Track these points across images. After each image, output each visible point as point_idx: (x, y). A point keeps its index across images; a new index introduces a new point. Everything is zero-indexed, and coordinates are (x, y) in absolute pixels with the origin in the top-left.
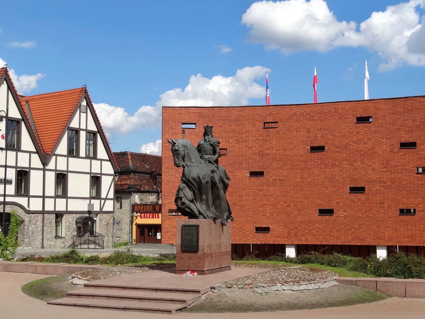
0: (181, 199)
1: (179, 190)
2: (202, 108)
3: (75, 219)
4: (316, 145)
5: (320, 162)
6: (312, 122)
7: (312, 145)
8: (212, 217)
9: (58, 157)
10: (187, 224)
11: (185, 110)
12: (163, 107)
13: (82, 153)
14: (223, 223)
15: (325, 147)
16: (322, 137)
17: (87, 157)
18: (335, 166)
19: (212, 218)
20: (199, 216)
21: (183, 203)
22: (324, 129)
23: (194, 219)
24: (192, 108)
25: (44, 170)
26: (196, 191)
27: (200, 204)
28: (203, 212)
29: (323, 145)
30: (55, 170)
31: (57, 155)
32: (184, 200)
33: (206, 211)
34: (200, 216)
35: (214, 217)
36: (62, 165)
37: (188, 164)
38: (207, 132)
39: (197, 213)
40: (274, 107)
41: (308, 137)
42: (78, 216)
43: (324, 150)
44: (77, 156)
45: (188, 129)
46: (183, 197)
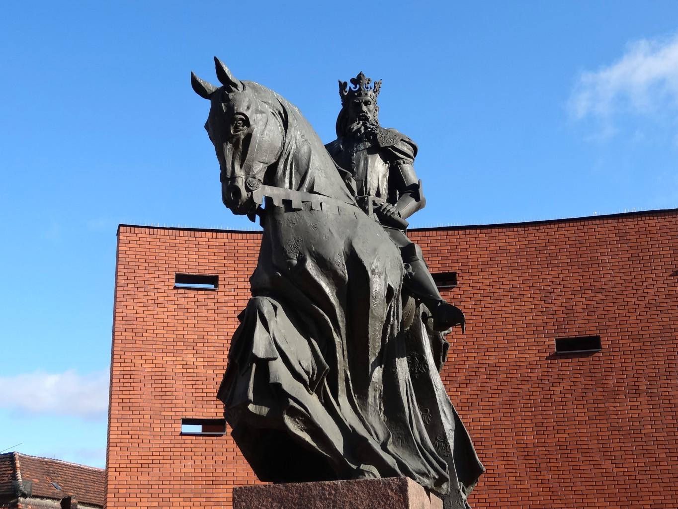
0: (264, 364)
1: (249, 318)
2: (237, 234)
4: (574, 334)
5: (589, 382)
6: (555, 271)
7: (562, 335)
11: (187, 238)
12: (120, 225)
15: (602, 339)
16: (589, 310)
18: (638, 392)
19: (427, 481)
21: (274, 394)
22: (594, 290)
23: (339, 482)
24: (207, 233)
26: (339, 334)
29: (594, 333)
32: (279, 372)
34: (363, 467)
37: (296, 197)
38: (359, 105)
40: (442, 233)
41: (547, 313)
43: (599, 346)
45: (196, 292)
46: (275, 359)
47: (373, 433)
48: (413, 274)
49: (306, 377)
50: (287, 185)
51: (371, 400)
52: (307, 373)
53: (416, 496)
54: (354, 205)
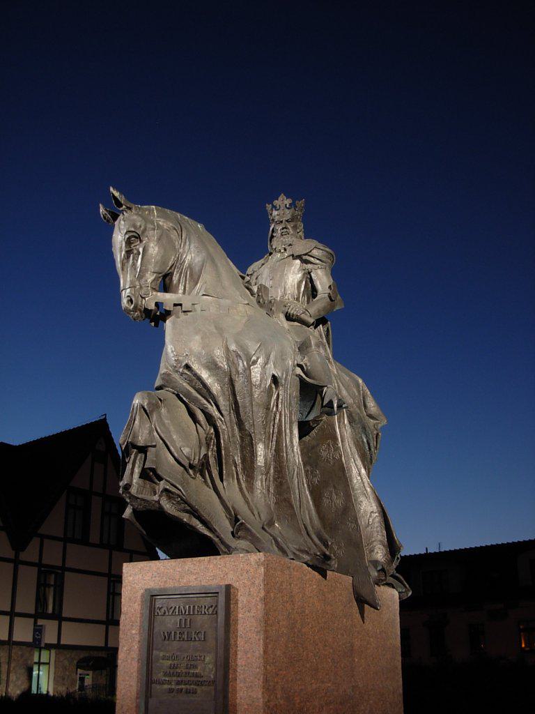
3: (75, 662)
8: (307, 553)
9: (46, 541)
10: (170, 584)
13: (94, 537)
14: (364, 592)
17: (101, 545)
19: (306, 557)
20: (233, 543)
25: (16, 562)
27: (241, 489)
28: (253, 522)
30: (39, 565)
31: (43, 537)
33: (271, 523)
35: (314, 550)
36: (52, 556)
39: (224, 526)
42: (83, 655)
44: (84, 541)
47: (256, 513)
48: (308, 364)
49: (186, 463)
50: (181, 291)
51: (258, 484)
52: (188, 458)
53: (282, 571)
54: (248, 304)
